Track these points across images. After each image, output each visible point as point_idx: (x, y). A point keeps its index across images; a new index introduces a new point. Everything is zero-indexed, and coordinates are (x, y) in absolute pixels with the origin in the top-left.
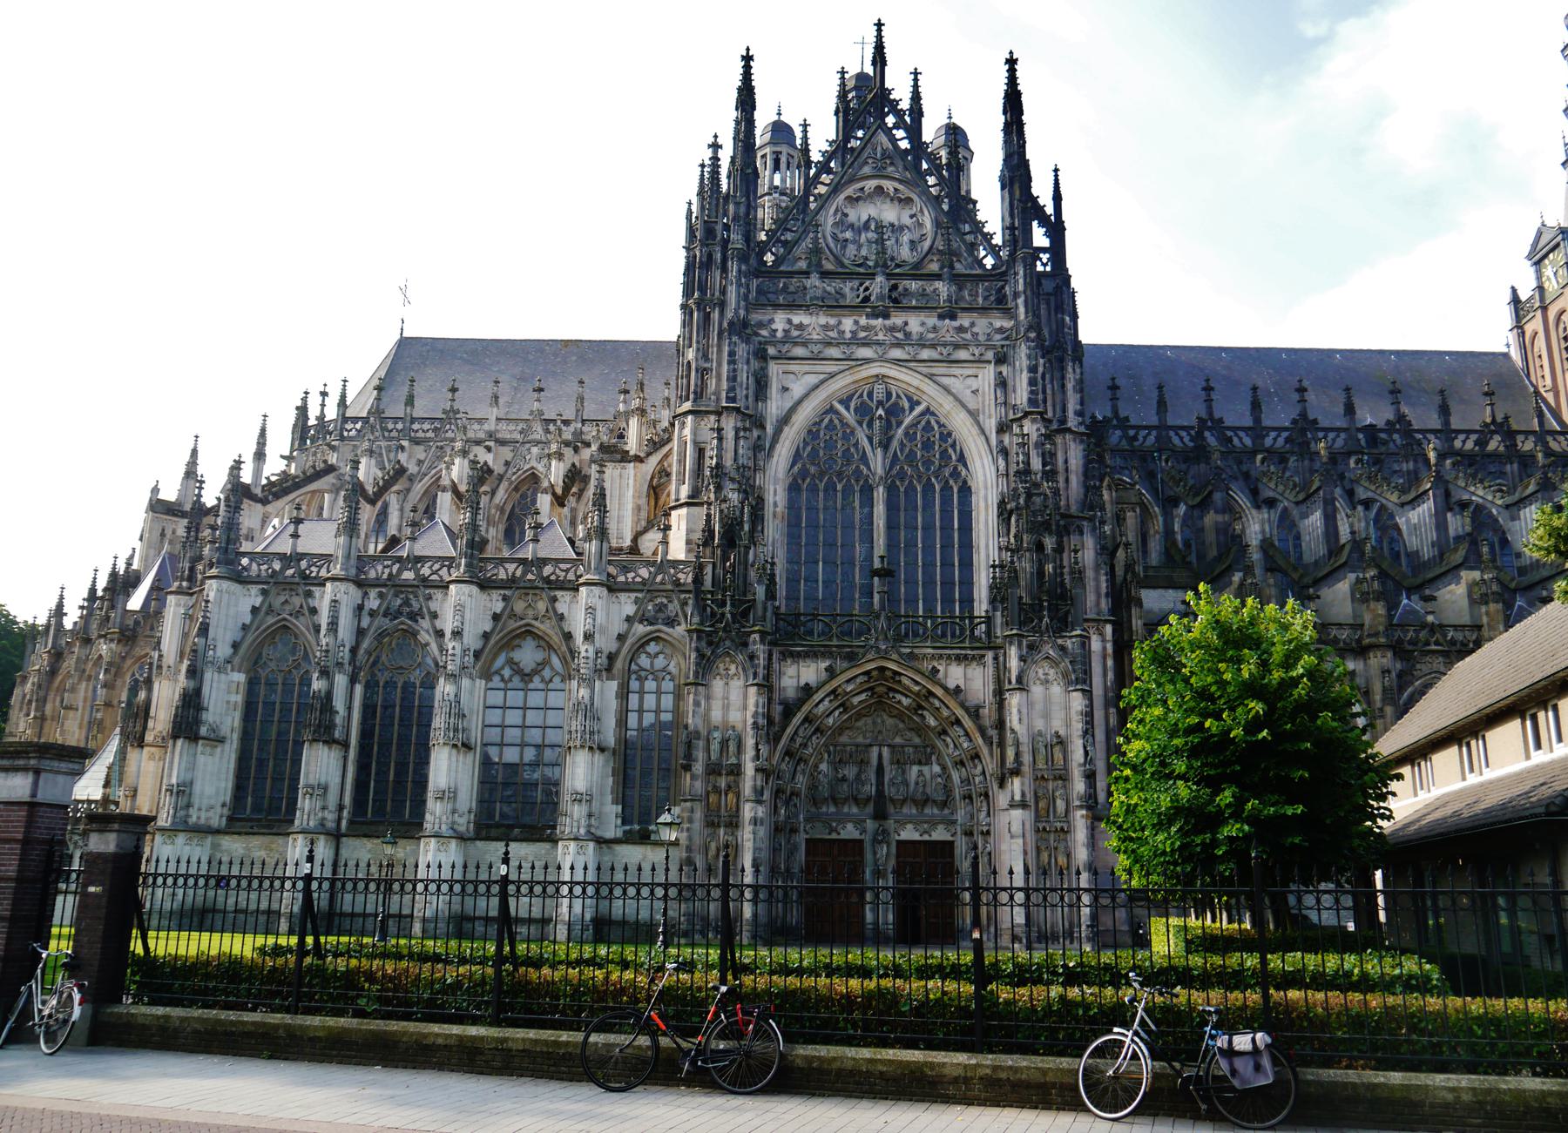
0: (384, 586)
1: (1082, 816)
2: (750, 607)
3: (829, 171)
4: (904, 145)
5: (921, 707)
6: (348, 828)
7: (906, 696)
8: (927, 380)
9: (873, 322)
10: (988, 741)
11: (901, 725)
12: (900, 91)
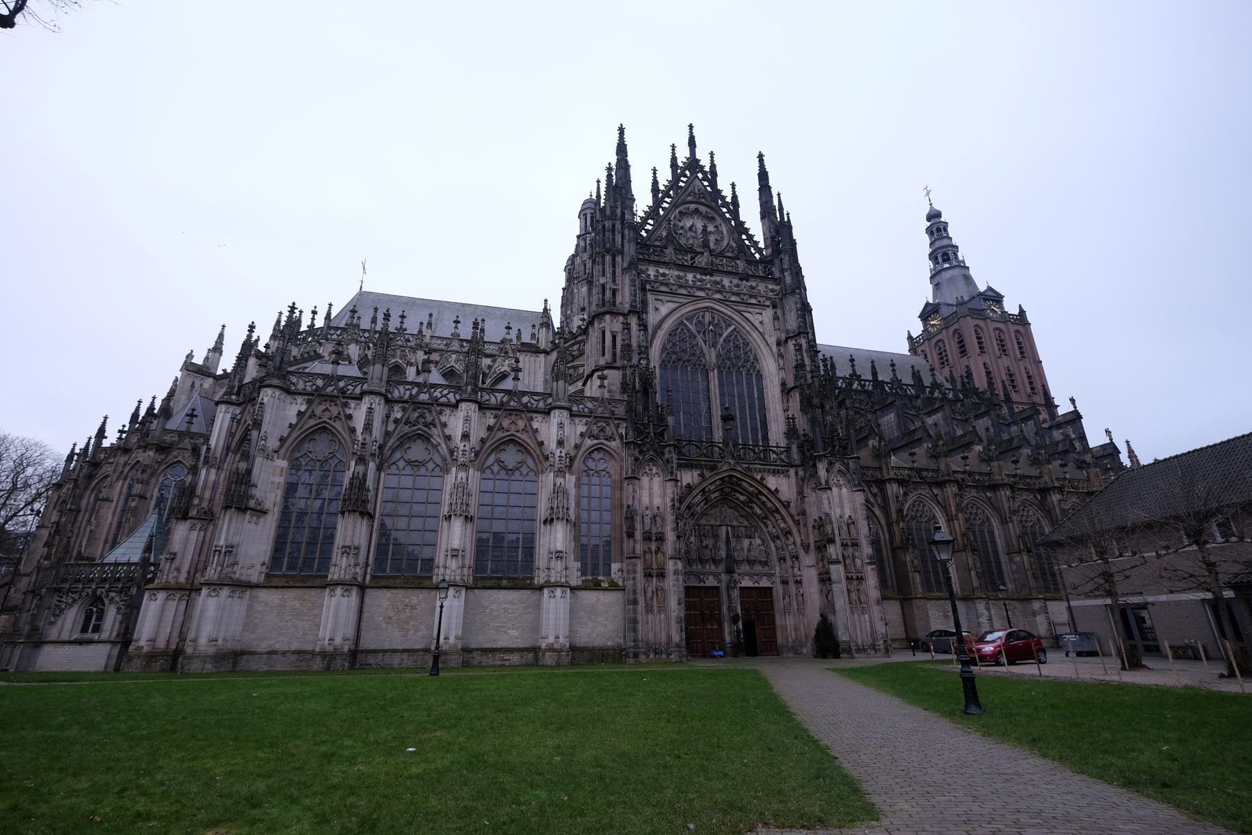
0: (406, 402)
1: (873, 569)
2: (664, 430)
3: (669, 196)
4: (709, 189)
6: (370, 581)
7: (742, 494)
9: (704, 277)
10: (797, 523)
11: (736, 514)
12: (705, 163)
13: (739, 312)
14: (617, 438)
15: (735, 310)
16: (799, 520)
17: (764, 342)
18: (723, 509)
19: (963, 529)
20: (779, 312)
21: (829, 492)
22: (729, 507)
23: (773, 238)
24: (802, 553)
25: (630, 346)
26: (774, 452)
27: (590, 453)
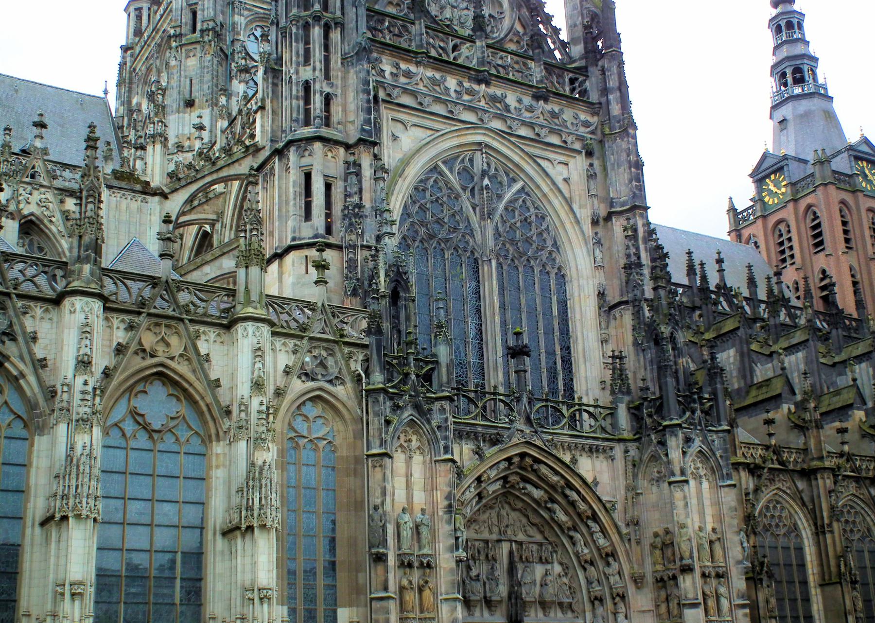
1: (745, 615)
2: (433, 369)
7: (537, 487)
8: (526, 158)
9: (476, 87)
11: (524, 520)
13: (531, 157)
14: (348, 379)
15: (527, 153)
16: (629, 534)
17: (571, 216)
18: (503, 513)
19: (839, 549)
20: (596, 163)
21: (686, 488)
22: (514, 510)
23: (586, 27)
24: (631, 589)
25: (360, 206)
26: (591, 415)
27: (299, 407)
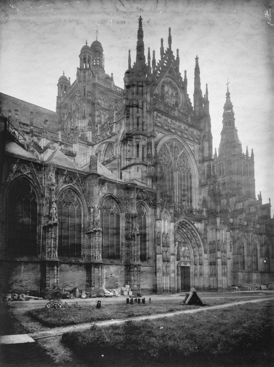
5: (188, 232)
10: (203, 242)
11: (181, 237)
22: (179, 234)
